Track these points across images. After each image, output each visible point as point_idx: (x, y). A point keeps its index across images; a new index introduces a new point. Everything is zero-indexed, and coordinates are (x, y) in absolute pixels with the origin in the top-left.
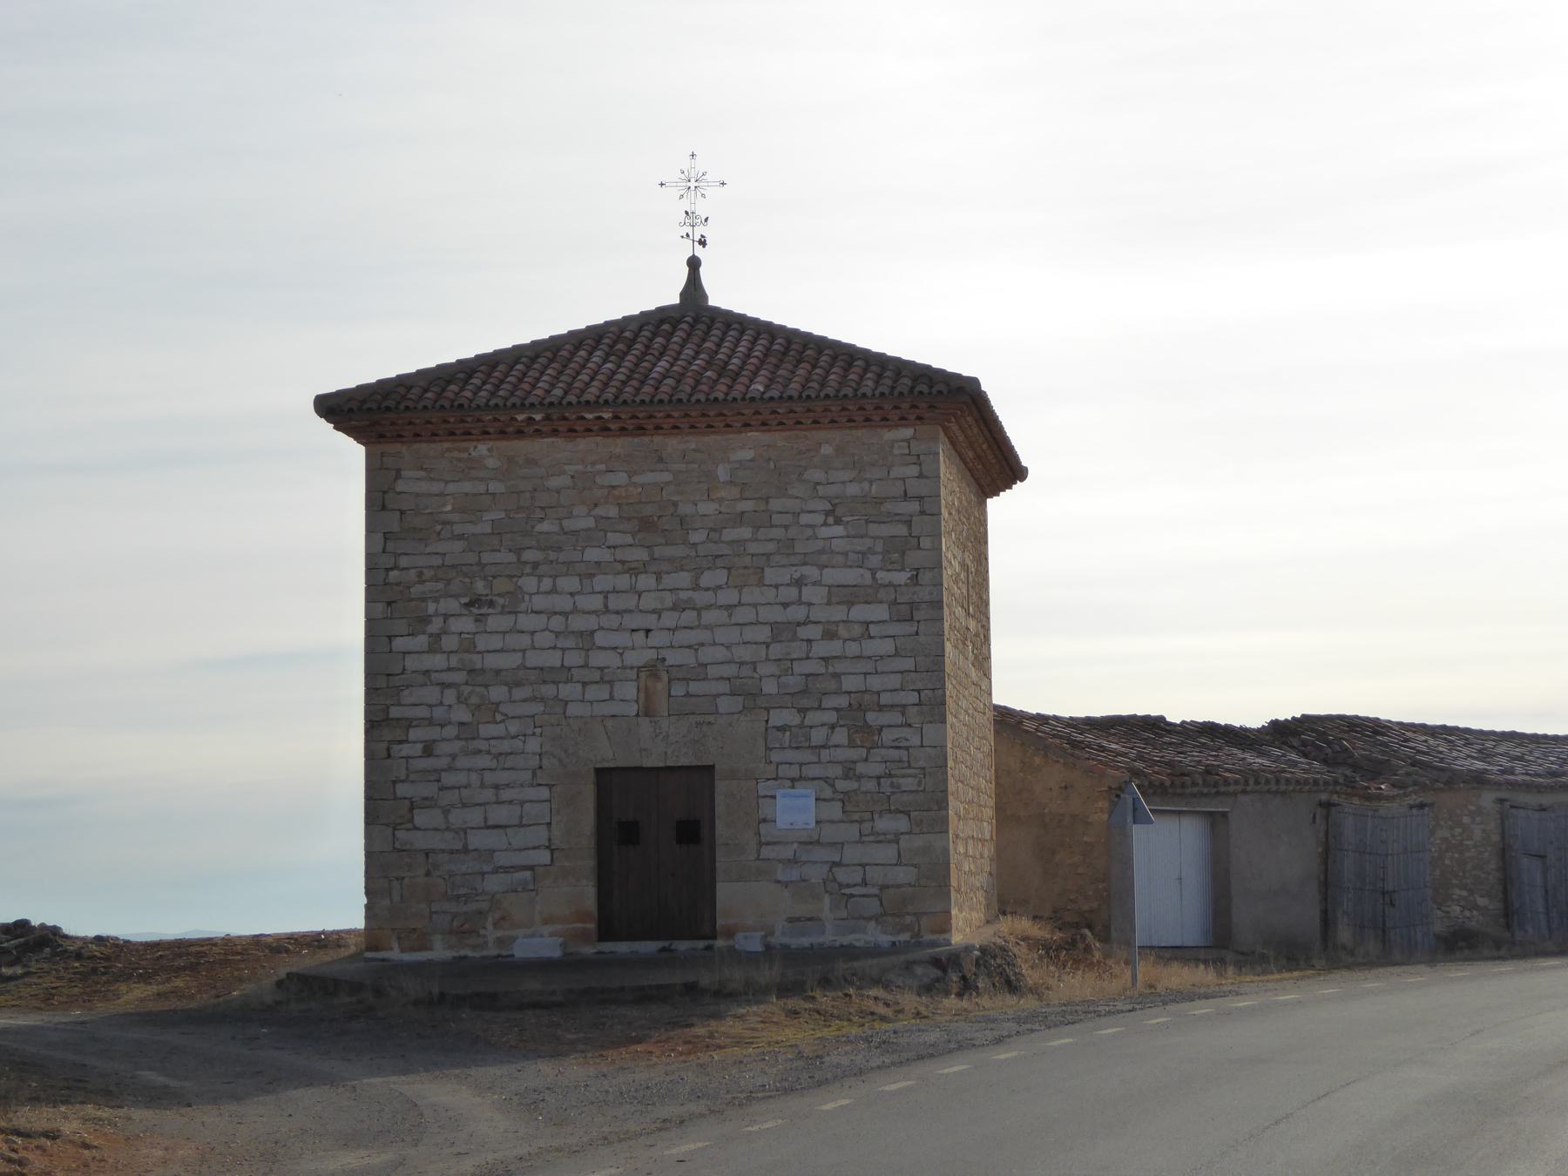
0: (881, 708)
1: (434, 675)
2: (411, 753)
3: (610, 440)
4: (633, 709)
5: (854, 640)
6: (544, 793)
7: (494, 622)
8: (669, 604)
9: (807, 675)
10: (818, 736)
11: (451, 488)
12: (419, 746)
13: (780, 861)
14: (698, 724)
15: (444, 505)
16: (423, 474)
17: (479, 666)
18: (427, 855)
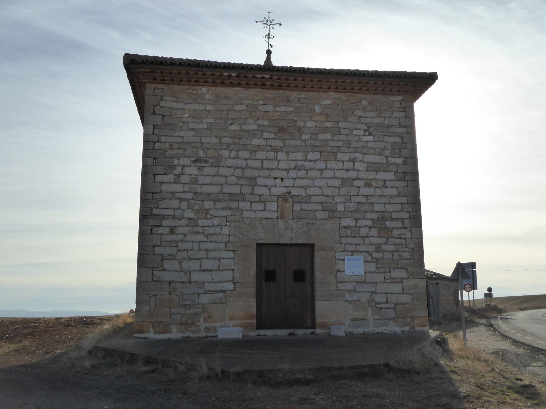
0: (392, 220)
1: (176, 195)
2: (163, 232)
3: (265, 91)
4: (275, 215)
5: (379, 188)
6: (231, 254)
7: (206, 171)
9: (358, 203)
10: (364, 232)
11: (188, 106)
12: (168, 229)
13: (347, 291)
14: (307, 224)
15: (184, 114)
16: (174, 99)
17: (199, 191)
18: (170, 284)
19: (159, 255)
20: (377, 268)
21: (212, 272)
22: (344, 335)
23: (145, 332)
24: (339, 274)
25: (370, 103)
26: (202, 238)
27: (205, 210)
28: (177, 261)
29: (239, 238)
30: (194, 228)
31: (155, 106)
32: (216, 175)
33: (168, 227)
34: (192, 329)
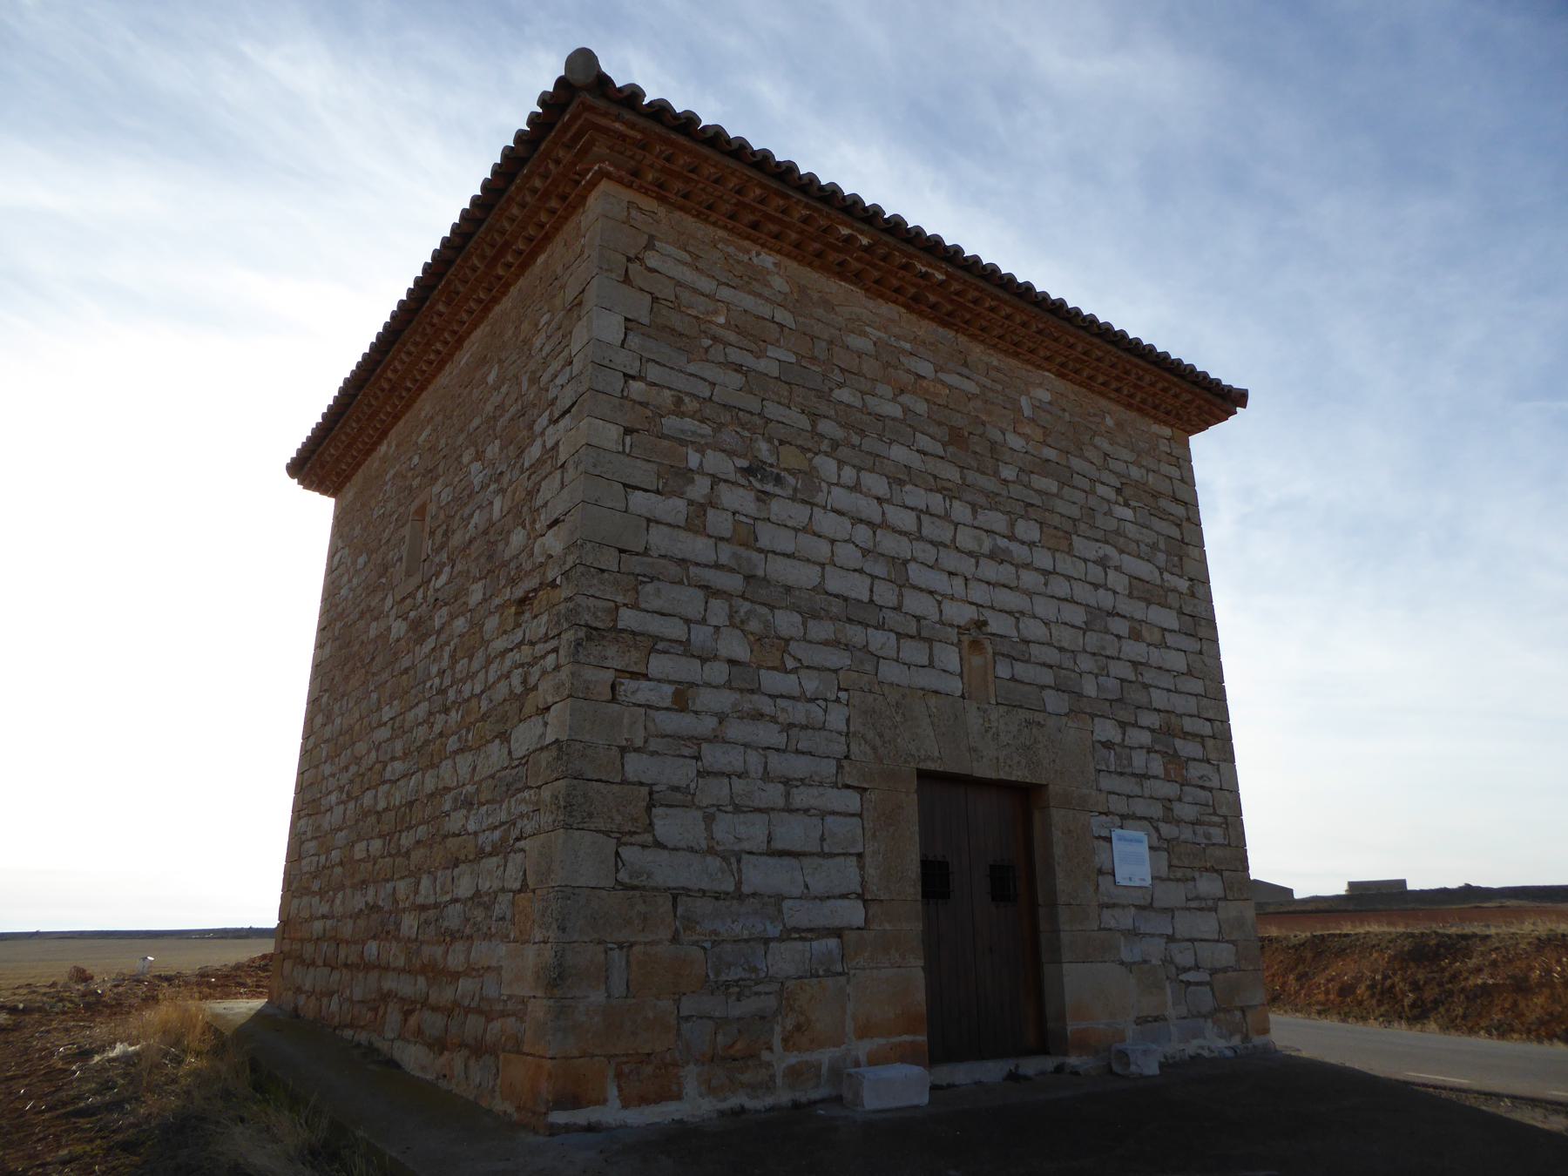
1: (692, 570)
2: (654, 699)
3: (913, 317)
4: (956, 686)
6: (852, 801)
7: (778, 508)
8: (986, 549)
9: (1122, 680)
12: (669, 690)
14: (1028, 723)
15: (716, 312)
17: (760, 573)
18: (675, 898)
19: (641, 784)
20: (1170, 866)
21: (806, 861)
22: (1157, 1072)
23: (590, 1103)
24: (1104, 882)
25: (1120, 425)
26: (769, 735)
27: (779, 638)
28: (699, 814)
29: (874, 749)
30: (748, 696)
31: (629, 260)
32: (805, 530)
33: (670, 682)
34: (746, 1077)
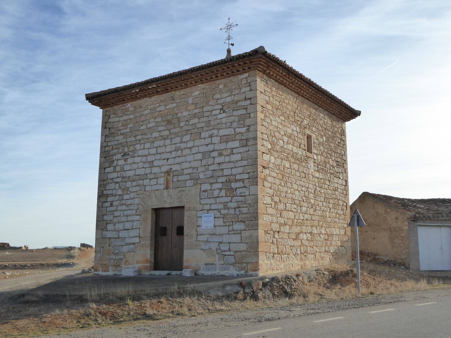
0: (236, 181)
3: (160, 96)
4: (162, 187)
5: (228, 155)
6: (138, 218)
7: (130, 161)
8: (174, 149)
10: (216, 193)
11: (121, 119)
13: (203, 241)
14: (180, 191)
16: (115, 115)
17: (125, 176)
24: (199, 229)
25: (225, 86)
26: (124, 207)
